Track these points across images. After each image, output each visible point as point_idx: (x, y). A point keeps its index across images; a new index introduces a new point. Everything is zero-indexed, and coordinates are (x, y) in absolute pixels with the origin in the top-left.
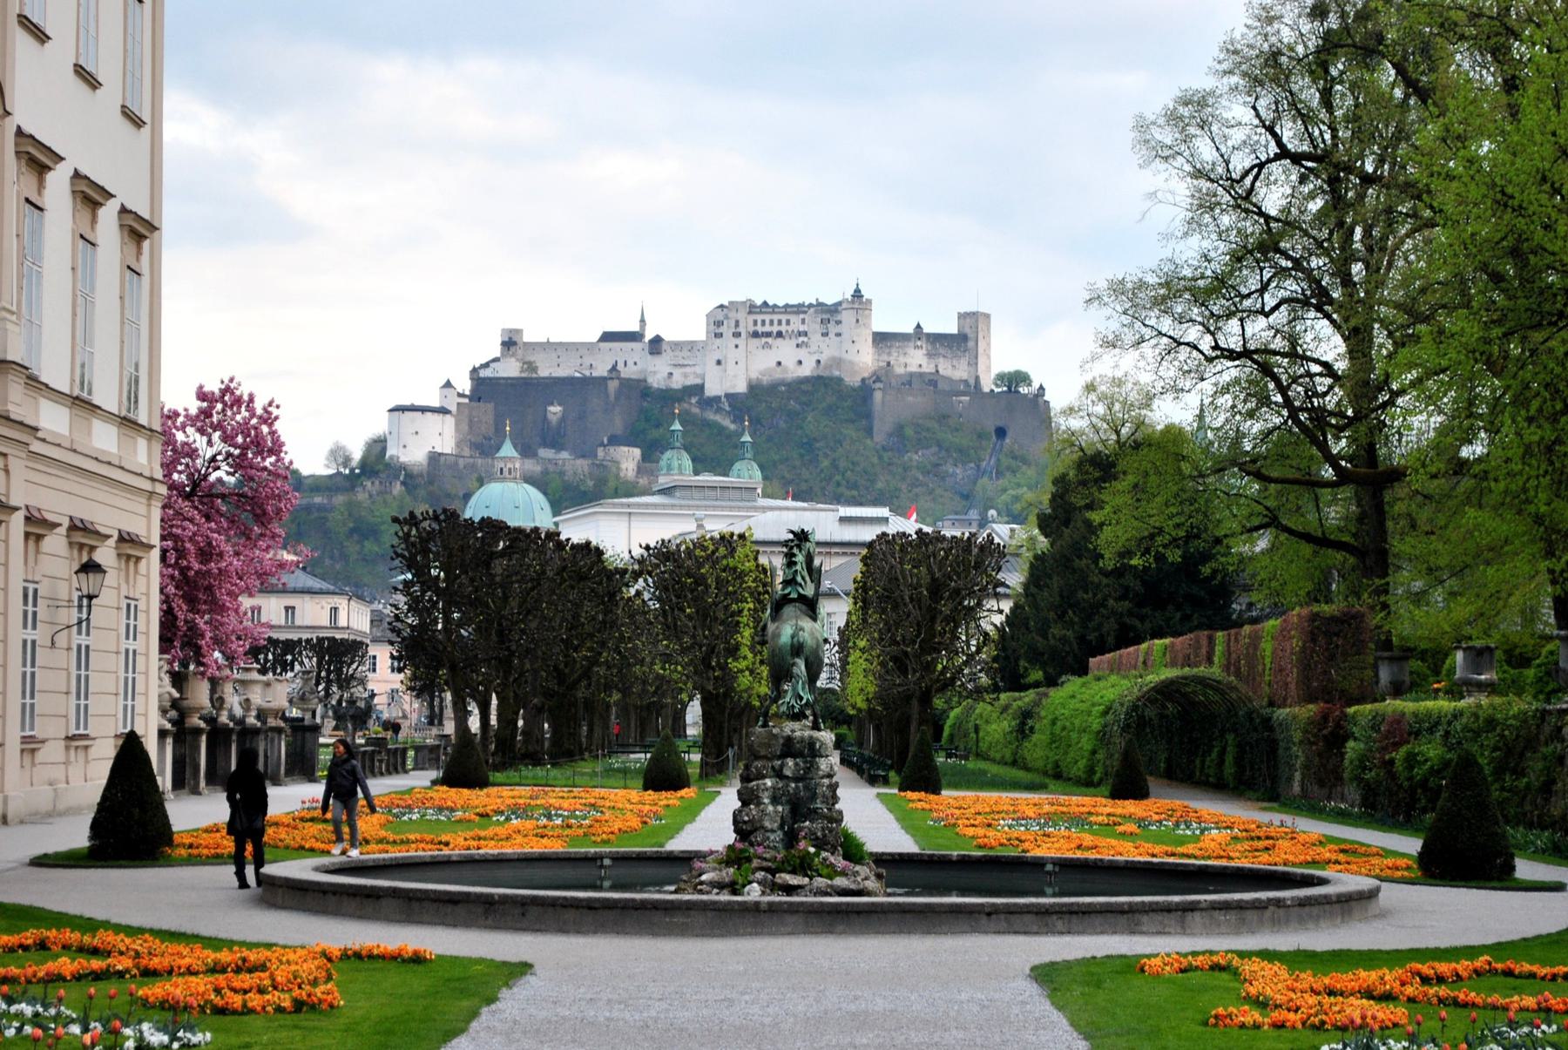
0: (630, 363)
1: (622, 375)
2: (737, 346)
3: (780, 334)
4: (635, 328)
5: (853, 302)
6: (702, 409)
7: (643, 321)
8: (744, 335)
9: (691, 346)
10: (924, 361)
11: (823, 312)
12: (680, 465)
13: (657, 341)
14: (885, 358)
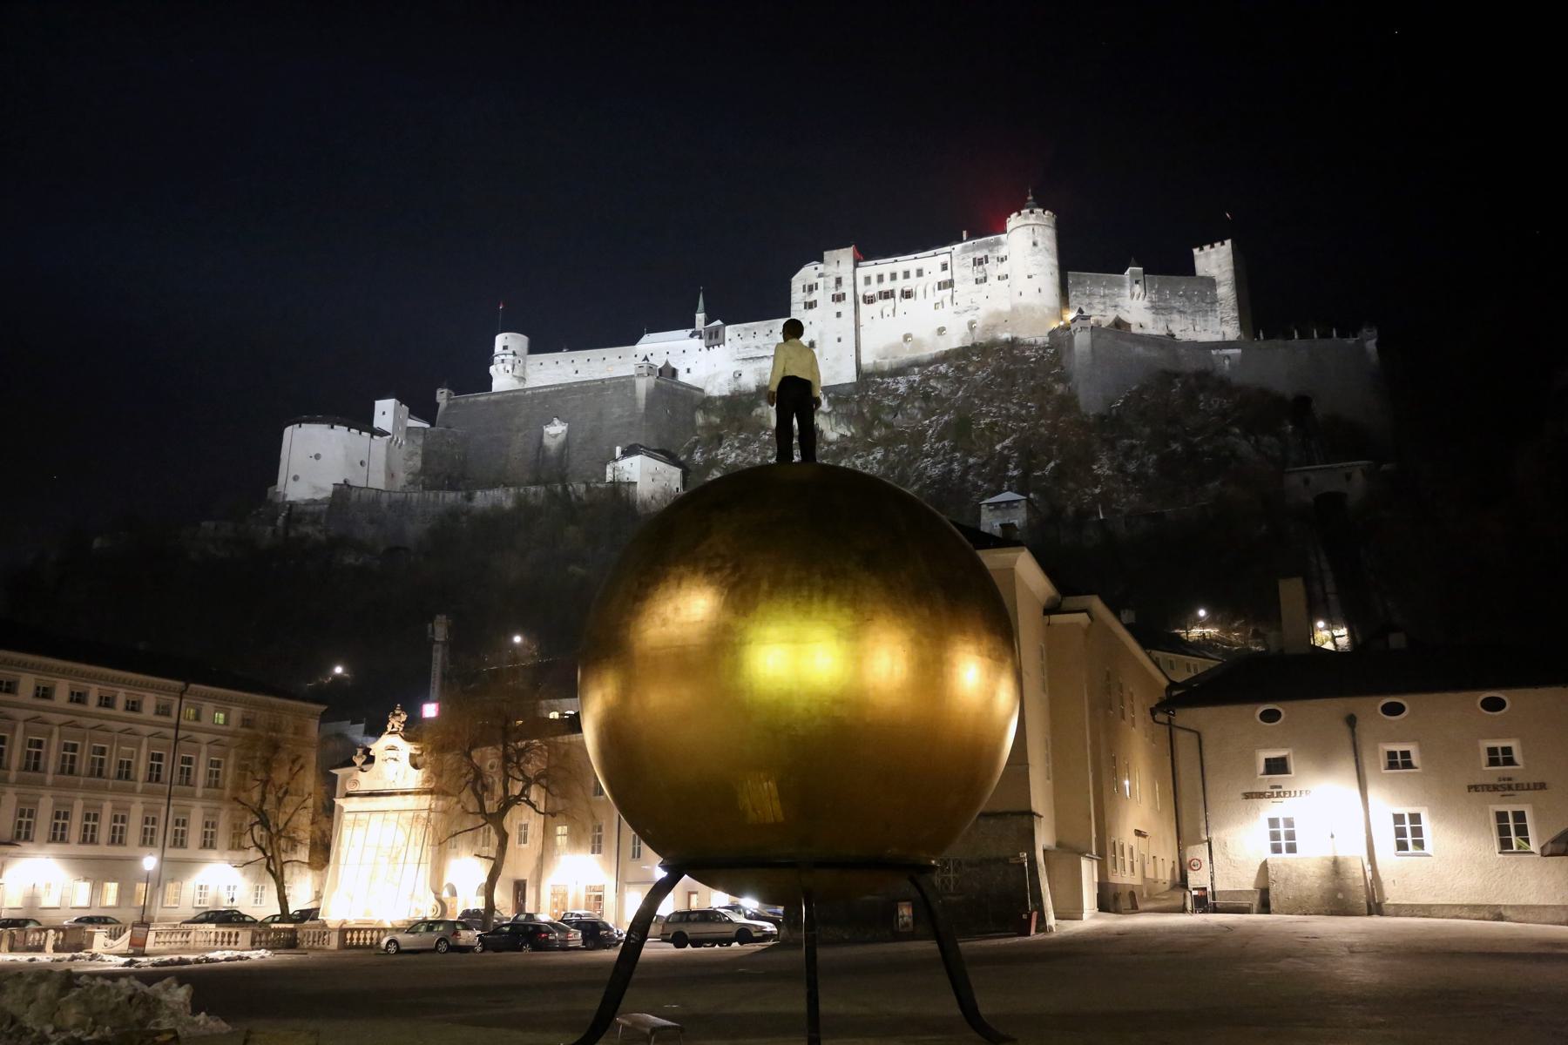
2: (839, 315)
3: (907, 295)
8: (850, 298)
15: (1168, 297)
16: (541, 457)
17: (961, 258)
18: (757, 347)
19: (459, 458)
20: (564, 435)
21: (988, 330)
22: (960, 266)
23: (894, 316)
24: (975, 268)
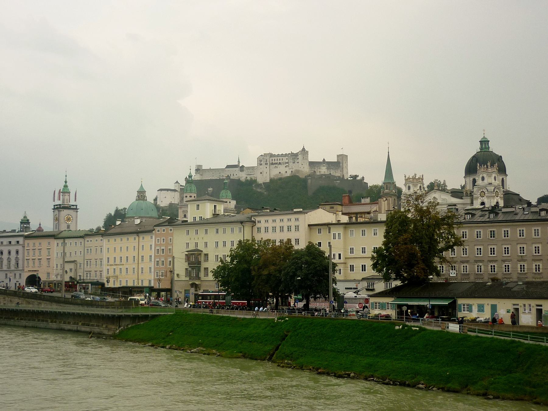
0: (235, 174)
1: (231, 178)
2: (266, 168)
3: (280, 163)
5: (302, 152)
7: (239, 161)
8: (268, 164)
9: (253, 168)
10: (326, 171)
11: (293, 156)
12: (191, 189)
13: (243, 166)
14: (313, 170)
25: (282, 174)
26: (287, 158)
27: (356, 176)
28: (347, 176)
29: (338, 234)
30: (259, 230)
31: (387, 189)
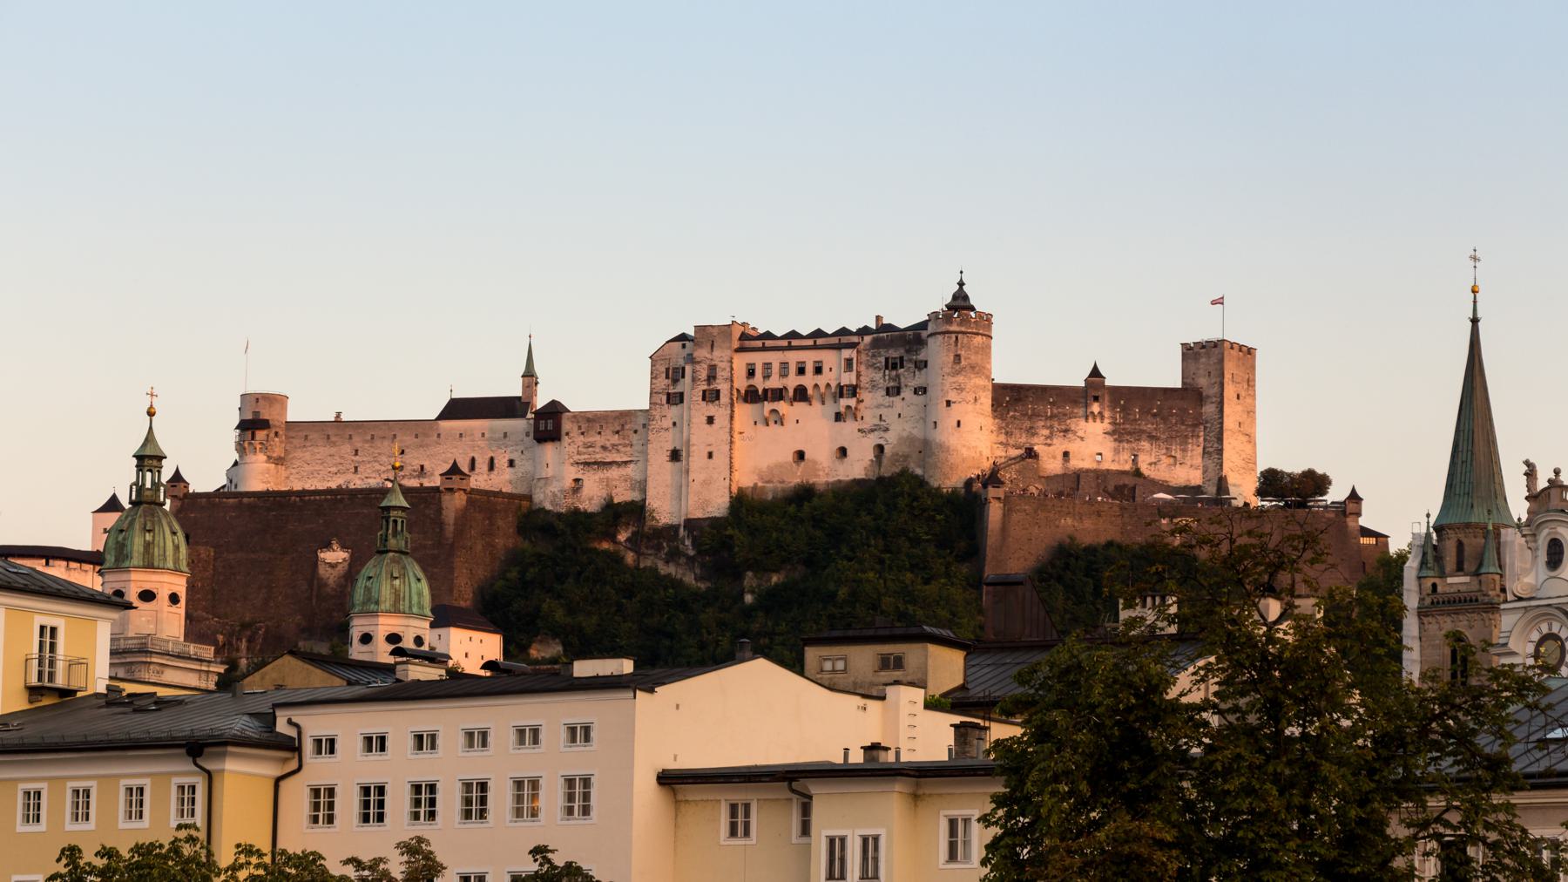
0: (502, 462)
2: (710, 420)
3: (801, 394)
4: (512, 388)
6: (639, 554)
7: (529, 375)
9: (620, 421)
10: (1107, 446)
11: (890, 344)
12: (148, 546)
13: (554, 411)
14: (1023, 440)
15: (1138, 416)
16: (314, 593)
17: (870, 354)
18: (604, 448)
19: (203, 586)
20: (346, 564)
21: (897, 461)
22: (868, 366)
23: (782, 424)
24: (887, 372)
25: (815, 462)
26: (849, 362)
27: (1315, 483)
28: (1244, 490)
29: (858, 843)
30: (323, 803)
31: (1460, 568)
